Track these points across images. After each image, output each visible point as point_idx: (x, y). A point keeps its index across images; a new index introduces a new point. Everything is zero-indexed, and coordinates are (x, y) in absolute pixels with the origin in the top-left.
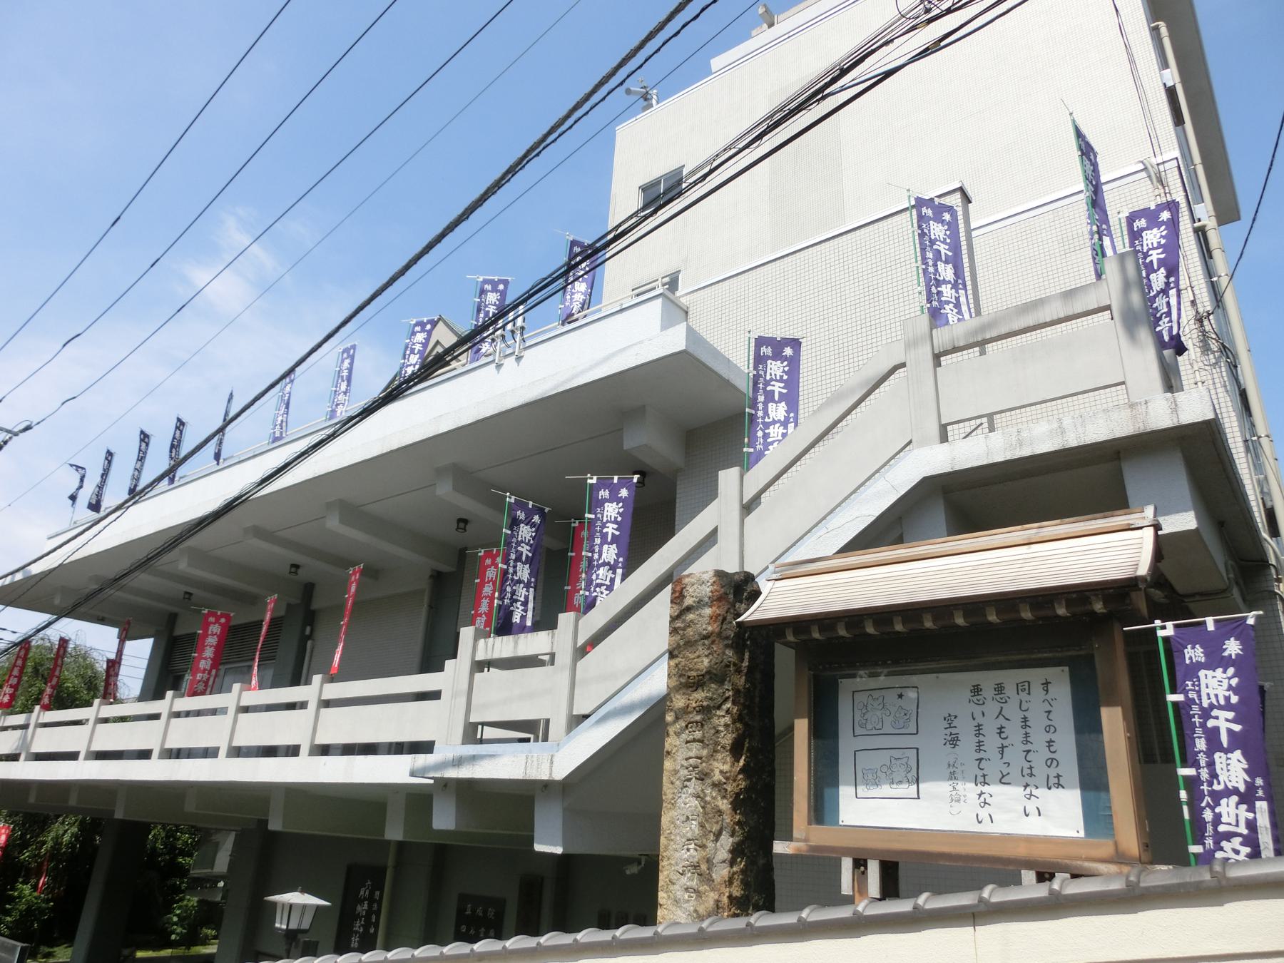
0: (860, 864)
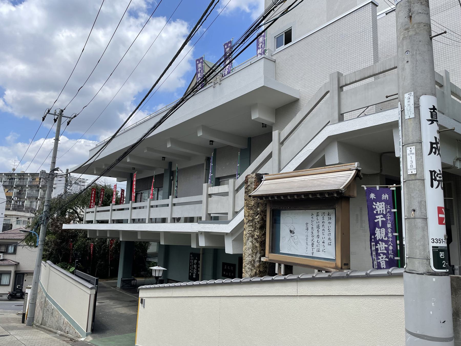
0: (280, 265)
